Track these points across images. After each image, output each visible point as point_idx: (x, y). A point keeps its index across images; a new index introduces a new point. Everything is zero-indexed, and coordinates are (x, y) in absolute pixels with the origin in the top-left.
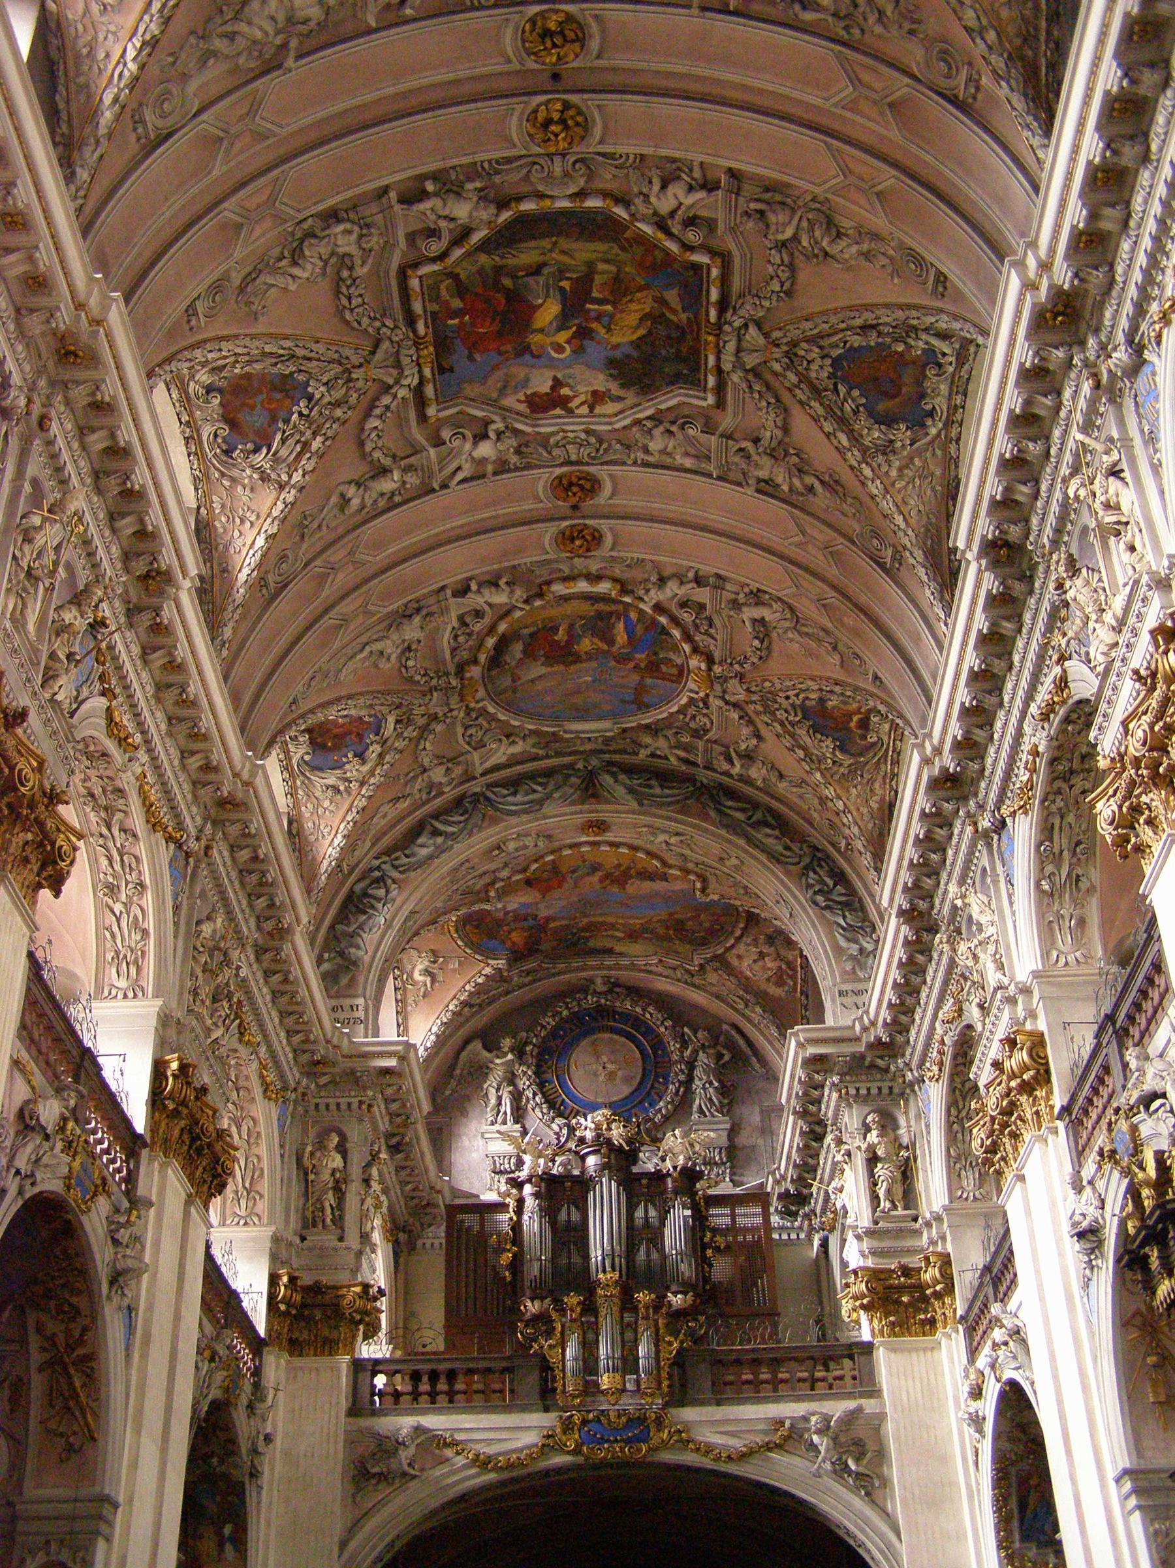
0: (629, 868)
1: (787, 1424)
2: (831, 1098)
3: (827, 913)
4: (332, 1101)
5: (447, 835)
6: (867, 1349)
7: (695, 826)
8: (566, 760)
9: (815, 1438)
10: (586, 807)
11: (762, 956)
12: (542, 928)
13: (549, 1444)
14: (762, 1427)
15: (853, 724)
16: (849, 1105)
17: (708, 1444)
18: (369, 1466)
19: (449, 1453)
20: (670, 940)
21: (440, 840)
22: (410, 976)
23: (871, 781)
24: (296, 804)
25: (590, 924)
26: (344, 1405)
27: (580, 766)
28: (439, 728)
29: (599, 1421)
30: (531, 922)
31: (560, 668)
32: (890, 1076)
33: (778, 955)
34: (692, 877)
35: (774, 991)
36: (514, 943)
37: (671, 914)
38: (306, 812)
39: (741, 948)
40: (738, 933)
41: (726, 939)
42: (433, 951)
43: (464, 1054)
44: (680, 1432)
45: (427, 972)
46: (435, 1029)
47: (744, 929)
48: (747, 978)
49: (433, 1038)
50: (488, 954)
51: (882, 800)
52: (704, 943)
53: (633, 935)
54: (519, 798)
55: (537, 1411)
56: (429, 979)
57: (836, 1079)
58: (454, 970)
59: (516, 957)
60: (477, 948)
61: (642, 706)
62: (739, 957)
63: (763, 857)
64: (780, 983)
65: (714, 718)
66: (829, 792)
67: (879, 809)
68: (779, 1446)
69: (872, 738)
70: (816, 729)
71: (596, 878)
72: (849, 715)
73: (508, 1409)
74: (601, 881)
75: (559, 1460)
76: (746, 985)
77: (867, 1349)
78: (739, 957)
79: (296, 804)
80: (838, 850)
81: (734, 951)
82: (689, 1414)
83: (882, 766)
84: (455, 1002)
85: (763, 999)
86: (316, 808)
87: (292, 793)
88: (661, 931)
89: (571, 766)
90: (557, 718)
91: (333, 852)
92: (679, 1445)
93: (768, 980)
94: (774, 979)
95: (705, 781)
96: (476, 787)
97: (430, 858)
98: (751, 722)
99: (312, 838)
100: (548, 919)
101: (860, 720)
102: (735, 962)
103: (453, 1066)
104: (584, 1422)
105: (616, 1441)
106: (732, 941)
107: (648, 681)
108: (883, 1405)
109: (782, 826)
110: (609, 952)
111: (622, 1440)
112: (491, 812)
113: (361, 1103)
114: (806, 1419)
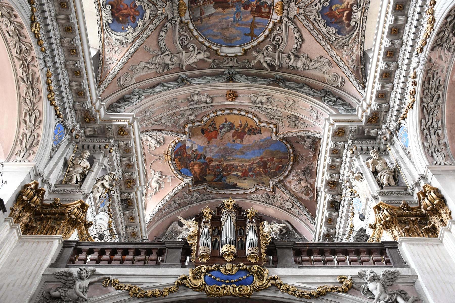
0: (245, 127)
1: (349, 278)
2: (347, 154)
3: (335, 107)
4: (91, 145)
5: (168, 87)
6: (394, 245)
7: (274, 89)
8: (221, 70)
9: (371, 286)
10: (228, 84)
11: (300, 180)
12: (207, 165)
13: (182, 284)
14: (331, 280)
15: (344, 18)
16: (358, 157)
17: (293, 286)
18: (51, 292)
19: (112, 289)
20: (261, 175)
21: (165, 88)
22: (150, 184)
23: (352, 48)
24: (103, 47)
25: (227, 166)
26: (49, 261)
27: (227, 72)
28: (169, 25)
29: (219, 270)
30: (202, 161)
31: (220, 10)
32: (378, 141)
33: (307, 181)
34: (272, 126)
35: (305, 197)
36: (195, 172)
37: (262, 158)
38: (107, 50)
39: (291, 177)
40: (290, 168)
41: (285, 172)
42: (161, 172)
43: (170, 227)
44: (274, 279)
45: (157, 182)
46: (158, 206)
47: (293, 166)
48: (293, 192)
49: (157, 210)
50: (184, 175)
51: (357, 56)
52: (274, 175)
53: (245, 175)
54: (200, 80)
55: (177, 267)
56: (158, 185)
57: (350, 142)
58: (169, 183)
59: (196, 182)
60: (180, 173)
61: (253, 36)
62: (290, 182)
63: (304, 95)
64: (307, 194)
65: (283, 35)
66: (333, 53)
67: (357, 60)
68: (344, 291)
69: (353, 23)
70: (327, 24)
71: (230, 134)
72: (342, 13)
73: (157, 264)
74: (233, 136)
75: (189, 294)
76: (293, 194)
77: (394, 245)
78: (290, 182)
79: (103, 47)
80: (337, 87)
81: (288, 179)
82: (279, 272)
83: (357, 39)
84: (168, 196)
85: (300, 199)
86: (112, 50)
87: (102, 40)
88: (257, 169)
89: (223, 73)
90: (218, 44)
91: (117, 68)
92: (274, 288)
93: (302, 192)
94: (305, 192)
95: (278, 77)
96: (183, 75)
97: (160, 92)
98: (299, 31)
99: (108, 63)
100: (211, 160)
101: (347, 14)
102: (288, 185)
103: (165, 233)
104: (208, 271)
105: (230, 283)
106: (287, 173)
107: (257, 19)
108: (413, 271)
109: (311, 87)
110: (234, 186)
111: (234, 282)
112: (188, 83)
113: (106, 145)
114: (361, 276)
